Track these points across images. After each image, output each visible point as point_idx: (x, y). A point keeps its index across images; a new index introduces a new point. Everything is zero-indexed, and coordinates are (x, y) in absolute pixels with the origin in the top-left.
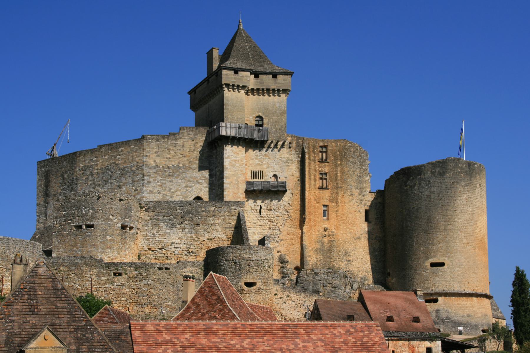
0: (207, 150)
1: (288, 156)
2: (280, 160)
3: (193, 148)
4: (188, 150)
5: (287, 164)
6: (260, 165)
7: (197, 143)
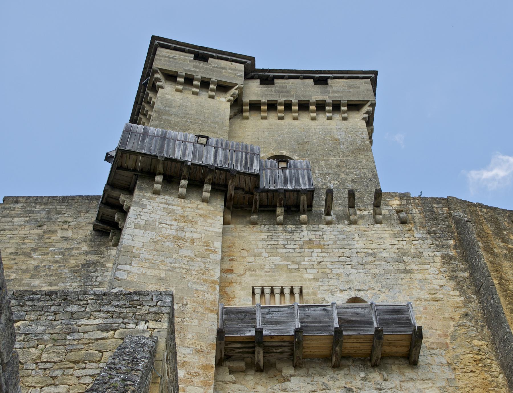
0: (85, 248)
1: (403, 244)
2: (367, 255)
3: (30, 244)
4: (13, 251)
5: (402, 267)
6: (291, 271)
7: (54, 232)
